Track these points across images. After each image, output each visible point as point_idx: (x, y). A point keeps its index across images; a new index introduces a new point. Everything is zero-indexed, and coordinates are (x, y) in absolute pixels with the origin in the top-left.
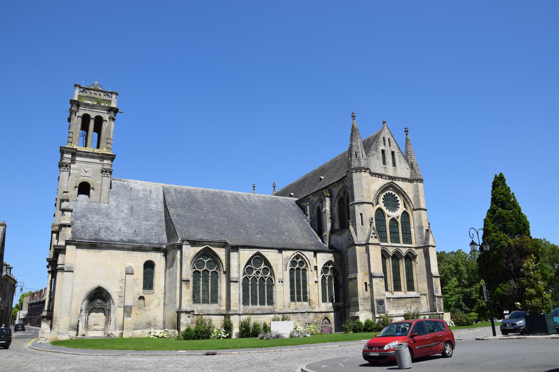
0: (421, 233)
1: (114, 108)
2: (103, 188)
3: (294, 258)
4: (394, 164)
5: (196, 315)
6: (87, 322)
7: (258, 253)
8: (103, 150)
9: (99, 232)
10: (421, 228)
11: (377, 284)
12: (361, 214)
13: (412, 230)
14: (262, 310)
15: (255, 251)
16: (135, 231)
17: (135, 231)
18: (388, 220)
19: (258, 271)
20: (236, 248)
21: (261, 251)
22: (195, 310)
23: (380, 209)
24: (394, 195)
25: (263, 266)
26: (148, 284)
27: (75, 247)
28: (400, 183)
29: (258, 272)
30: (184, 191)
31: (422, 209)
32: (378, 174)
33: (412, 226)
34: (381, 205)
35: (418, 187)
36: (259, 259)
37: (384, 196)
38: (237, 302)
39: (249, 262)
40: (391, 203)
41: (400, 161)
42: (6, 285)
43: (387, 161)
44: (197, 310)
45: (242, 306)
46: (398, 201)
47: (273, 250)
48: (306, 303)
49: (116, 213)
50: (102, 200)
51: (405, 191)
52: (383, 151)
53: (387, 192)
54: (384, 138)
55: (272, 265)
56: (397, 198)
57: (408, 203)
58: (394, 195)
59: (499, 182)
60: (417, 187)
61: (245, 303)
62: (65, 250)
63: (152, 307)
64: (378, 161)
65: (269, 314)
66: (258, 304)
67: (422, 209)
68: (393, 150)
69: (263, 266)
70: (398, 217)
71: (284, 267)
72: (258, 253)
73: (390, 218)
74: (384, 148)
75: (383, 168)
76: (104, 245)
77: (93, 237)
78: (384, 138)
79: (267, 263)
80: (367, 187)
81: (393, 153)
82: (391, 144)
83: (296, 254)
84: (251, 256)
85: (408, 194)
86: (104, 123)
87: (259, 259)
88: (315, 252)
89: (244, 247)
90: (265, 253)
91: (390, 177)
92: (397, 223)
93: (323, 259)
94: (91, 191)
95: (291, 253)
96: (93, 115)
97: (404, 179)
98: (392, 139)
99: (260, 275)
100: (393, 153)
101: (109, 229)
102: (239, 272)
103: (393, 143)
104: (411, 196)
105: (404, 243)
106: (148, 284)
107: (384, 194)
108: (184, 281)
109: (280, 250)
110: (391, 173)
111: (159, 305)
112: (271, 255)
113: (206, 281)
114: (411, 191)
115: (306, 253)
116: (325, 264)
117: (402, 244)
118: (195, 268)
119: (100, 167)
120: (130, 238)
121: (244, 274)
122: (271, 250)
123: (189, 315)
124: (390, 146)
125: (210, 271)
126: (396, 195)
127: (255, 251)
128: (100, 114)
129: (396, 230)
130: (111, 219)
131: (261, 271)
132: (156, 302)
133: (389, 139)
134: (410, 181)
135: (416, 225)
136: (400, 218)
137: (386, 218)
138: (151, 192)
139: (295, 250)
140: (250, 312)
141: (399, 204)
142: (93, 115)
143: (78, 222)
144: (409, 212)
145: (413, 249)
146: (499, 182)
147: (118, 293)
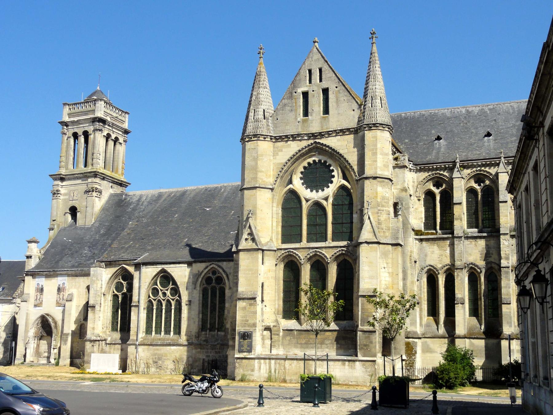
1: (96, 118)
4: (326, 111)
5: (109, 344)
7: (163, 271)
8: (89, 169)
11: (244, 308)
14: (164, 340)
15: (159, 268)
18: (305, 206)
20: (138, 266)
21: (166, 267)
22: (109, 339)
25: (171, 286)
27: (31, 277)
28: (332, 142)
29: (164, 294)
30: (178, 194)
31: (367, 178)
34: (298, 184)
37: (305, 168)
43: (310, 110)
47: (181, 265)
48: (223, 333)
50: (87, 222)
51: (341, 152)
52: (305, 95)
54: (310, 71)
55: (178, 284)
61: (148, 330)
64: (292, 115)
65: (169, 345)
68: (325, 86)
69: (171, 286)
70: (326, 199)
71: (193, 286)
72: (163, 271)
74: (305, 89)
75: (300, 124)
76: (52, 273)
78: (310, 71)
79: (174, 283)
80: (253, 163)
81: (326, 91)
83: (209, 268)
85: (345, 156)
86: (90, 136)
89: (146, 264)
91: (313, 136)
94: (78, 214)
96: (80, 132)
97: (341, 131)
98: (325, 68)
100: (326, 91)
103: (327, 73)
104: (352, 158)
105: (333, 240)
107: (305, 164)
108: (90, 307)
110: (315, 128)
117: (330, 243)
118: (114, 292)
119: (84, 188)
122: (177, 265)
123: (92, 344)
124: (321, 80)
126: (329, 162)
127: (159, 268)
128: (86, 129)
131: (168, 293)
133: (320, 70)
135: (359, 207)
136: (331, 200)
137: (304, 202)
140: (149, 343)
142: (80, 132)
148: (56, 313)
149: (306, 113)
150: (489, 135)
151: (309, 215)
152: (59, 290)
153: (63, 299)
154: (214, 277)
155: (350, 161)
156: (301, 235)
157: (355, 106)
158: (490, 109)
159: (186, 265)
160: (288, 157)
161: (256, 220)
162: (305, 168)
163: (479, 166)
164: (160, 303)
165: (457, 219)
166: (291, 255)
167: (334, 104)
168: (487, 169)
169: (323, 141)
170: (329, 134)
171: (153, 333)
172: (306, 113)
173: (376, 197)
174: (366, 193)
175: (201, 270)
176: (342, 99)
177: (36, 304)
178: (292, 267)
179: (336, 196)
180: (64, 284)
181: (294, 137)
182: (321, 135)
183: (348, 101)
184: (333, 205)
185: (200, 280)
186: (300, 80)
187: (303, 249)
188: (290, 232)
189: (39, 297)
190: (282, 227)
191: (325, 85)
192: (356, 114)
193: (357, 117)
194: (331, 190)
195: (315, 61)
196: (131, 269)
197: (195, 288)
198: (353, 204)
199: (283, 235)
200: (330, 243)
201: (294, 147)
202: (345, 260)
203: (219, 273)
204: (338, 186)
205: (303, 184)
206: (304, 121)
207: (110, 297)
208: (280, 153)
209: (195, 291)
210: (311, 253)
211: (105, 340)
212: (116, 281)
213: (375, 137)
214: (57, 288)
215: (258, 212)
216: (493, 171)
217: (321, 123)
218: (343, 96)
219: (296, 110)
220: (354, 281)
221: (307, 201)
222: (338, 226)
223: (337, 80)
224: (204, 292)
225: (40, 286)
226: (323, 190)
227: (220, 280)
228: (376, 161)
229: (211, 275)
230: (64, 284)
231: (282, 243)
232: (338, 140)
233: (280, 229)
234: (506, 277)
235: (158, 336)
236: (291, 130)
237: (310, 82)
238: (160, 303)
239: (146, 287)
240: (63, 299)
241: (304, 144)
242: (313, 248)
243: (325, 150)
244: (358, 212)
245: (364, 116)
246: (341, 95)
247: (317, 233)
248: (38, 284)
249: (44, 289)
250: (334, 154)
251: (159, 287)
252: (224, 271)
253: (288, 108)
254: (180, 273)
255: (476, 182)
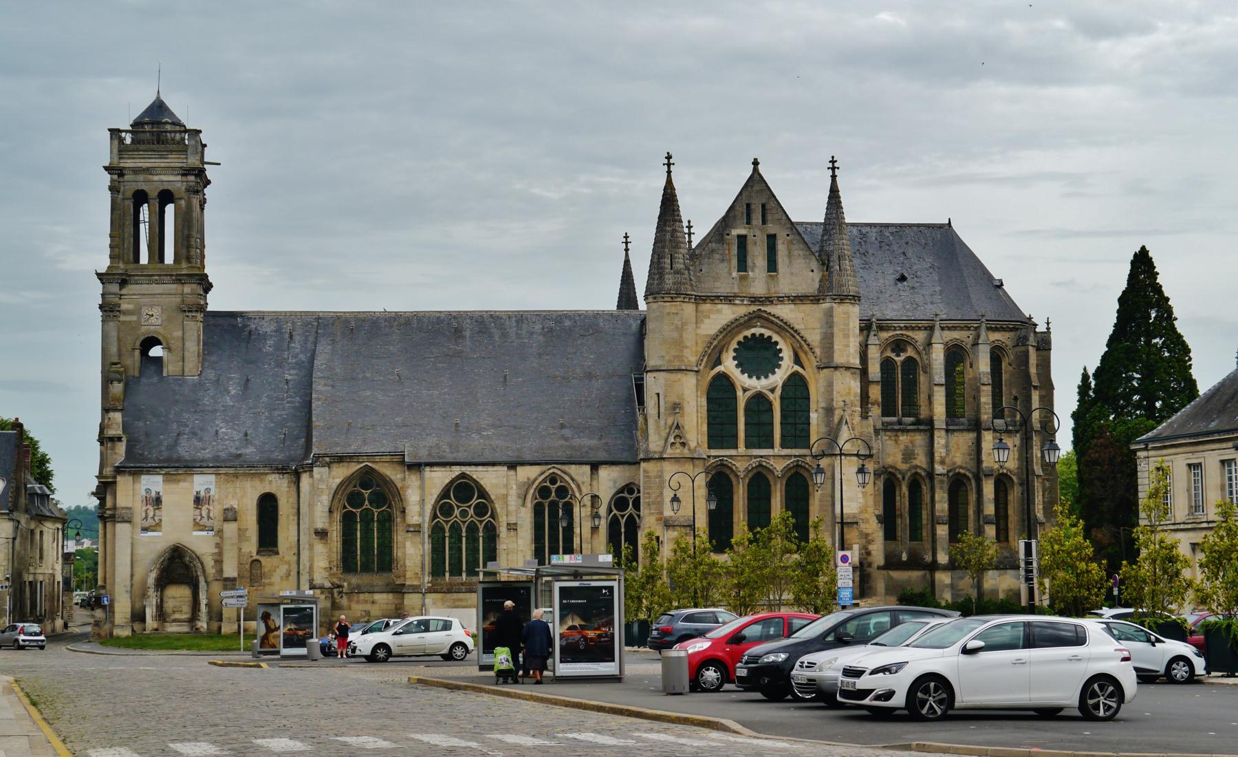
0: (828, 423)
1: (194, 169)
2: (188, 344)
3: (544, 481)
4: (772, 266)
6: (160, 607)
7: (463, 475)
9: (176, 443)
10: (829, 411)
12: (658, 395)
13: (814, 416)
15: (457, 470)
16: (246, 435)
17: (246, 435)
19: (465, 514)
20: (416, 467)
21: (467, 470)
23: (723, 378)
24: (770, 338)
26: (268, 538)
28: (784, 311)
29: (464, 513)
31: (836, 368)
32: (718, 297)
33: (813, 406)
34: (729, 365)
35: (831, 316)
36: (464, 489)
37: (739, 343)
38: (418, 570)
39: (445, 494)
40: (758, 355)
41: (790, 255)
42: (41, 532)
44: (349, 584)
45: (427, 578)
46: (780, 350)
47: (496, 468)
49: (212, 397)
50: (186, 370)
51: (797, 327)
53: (748, 333)
54: (748, 205)
56: (776, 343)
57: (806, 353)
58: (770, 338)
59: (1142, 263)
60: (829, 314)
61: (437, 570)
62: (115, 483)
63: (276, 578)
64: (722, 268)
66: (464, 575)
67: (836, 368)
68: (772, 232)
69: (474, 501)
70: (772, 391)
71: (520, 502)
73: (748, 394)
74: (743, 232)
75: (736, 282)
77: (165, 454)
78: (748, 205)
79: (483, 494)
81: (772, 239)
82: (769, 217)
84: (447, 481)
85: (803, 333)
87: (464, 489)
88: (595, 466)
89: (431, 465)
90: (477, 473)
91: (754, 300)
92: (770, 404)
93: (615, 482)
95: (536, 470)
96: (153, 193)
99: (469, 519)
100: (772, 239)
101: (195, 434)
102: (421, 514)
105: (783, 446)
106: (268, 538)
107: (740, 338)
109: (512, 466)
111: (288, 575)
112: (490, 479)
113: (367, 532)
114: (817, 325)
115: (573, 470)
116: (621, 490)
117: (777, 450)
118: (345, 507)
120: (233, 451)
121: (434, 516)
122: (490, 468)
124: (764, 222)
125: (376, 512)
127: (457, 470)
129: (764, 418)
130: (202, 411)
131: (471, 512)
132: (283, 569)
133: (763, 206)
134: (815, 299)
135: (823, 405)
136: (778, 392)
137: (740, 393)
138: (291, 336)
139: (547, 464)
141: (782, 359)
142: (153, 193)
143: (141, 424)
144: (809, 373)
145: (808, 459)
146: (1142, 263)
147: (213, 554)
148: (200, 543)
149: (743, 265)
150: (903, 278)
151: (747, 410)
152: (198, 501)
153: (209, 517)
154: (553, 488)
155: (809, 340)
156: (735, 436)
157: (814, 264)
158: (892, 233)
159: (505, 468)
160: (719, 327)
161: (682, 416)
162: (739, 343)
163: (901, 329)
164: (455, 529)
165: (873, 404)
166: (722, 465)
167: (786, 259)
168: (910, 333)
169: (769, 309)
170: (781, 300)
171: (447, 575)
172: (743, 265)
173: (849, 394)
174: (835, 388)
175: (533, 477)
176: (796, 253)
177: (146, 524)
178: (720, 483)
179: (784, 386)
180: (208, 490)
181: (729, 299)
182: (769, 300)
183: (805, 257)
184: (782, 398)
185: (532, 491)
186: (735, 217)
187: (741, 458)
188: (720, 433)
189: (151, 514)
190: (709, 424)
191: (771, 228)
192: (817, 276)
193: (817, 280)
194: (778, 378)
195: (757, 192)
196: (393, 474)
197: (524, 505)
198: (809, 399)
199: (709, 436)
200: (777, 450)
201: (726, 314)
202: (797, 473)
203: (563, 480)
204: (789, 373)
205: (737, 366)
206: (742, 278)
207: (337, 516)
208: (706, 321)
209: (523, 509)
210: (754, 463)
211: (339, 586)
212: (351, 489)
213: (847, 313)
214: (192, 499)
215: (685, 405)
216: (920, 336)
217: (767, 283)
218: (798, 251)
219: (730, 261)
220: (811, 502)
221: (745, 390)
222: (789, 427)
223: (789, 226)
224: (538, 511)
225: (153, 494)
226: (766, 377)
227: (562, 491)
228: (848, 346)
229: (548, 484)
230: (208, 490)
231: (709, 448)
232: (791, 310)
233: (705, 428)
234: (941, 488)
235: (456, 579)
236: (723, 288)
237: (749, 222)
238: (455, 529)
239: (433, 501)
240: (209, 517)
241: (741, 310)
242: (756, 457)
243: (772, 322)
244: (820, 411)
245: (831, 283)
246: (794, 247)
247: (760, 436)
248: (148, 491)
249: (163, 499)
250: (784, 328)
251: (453, 502)
252: (573, 479)
253: (717, 256)
254: (494, 481)
255: (893, 351)
